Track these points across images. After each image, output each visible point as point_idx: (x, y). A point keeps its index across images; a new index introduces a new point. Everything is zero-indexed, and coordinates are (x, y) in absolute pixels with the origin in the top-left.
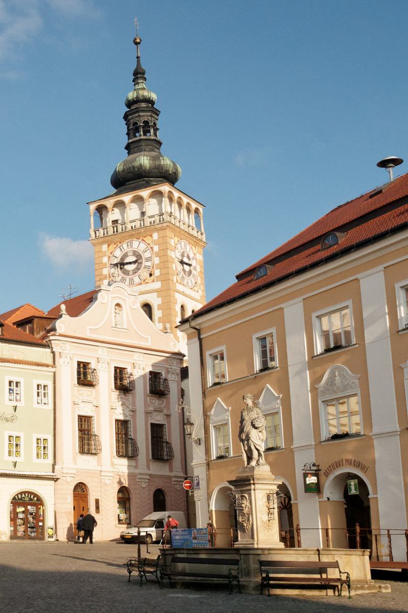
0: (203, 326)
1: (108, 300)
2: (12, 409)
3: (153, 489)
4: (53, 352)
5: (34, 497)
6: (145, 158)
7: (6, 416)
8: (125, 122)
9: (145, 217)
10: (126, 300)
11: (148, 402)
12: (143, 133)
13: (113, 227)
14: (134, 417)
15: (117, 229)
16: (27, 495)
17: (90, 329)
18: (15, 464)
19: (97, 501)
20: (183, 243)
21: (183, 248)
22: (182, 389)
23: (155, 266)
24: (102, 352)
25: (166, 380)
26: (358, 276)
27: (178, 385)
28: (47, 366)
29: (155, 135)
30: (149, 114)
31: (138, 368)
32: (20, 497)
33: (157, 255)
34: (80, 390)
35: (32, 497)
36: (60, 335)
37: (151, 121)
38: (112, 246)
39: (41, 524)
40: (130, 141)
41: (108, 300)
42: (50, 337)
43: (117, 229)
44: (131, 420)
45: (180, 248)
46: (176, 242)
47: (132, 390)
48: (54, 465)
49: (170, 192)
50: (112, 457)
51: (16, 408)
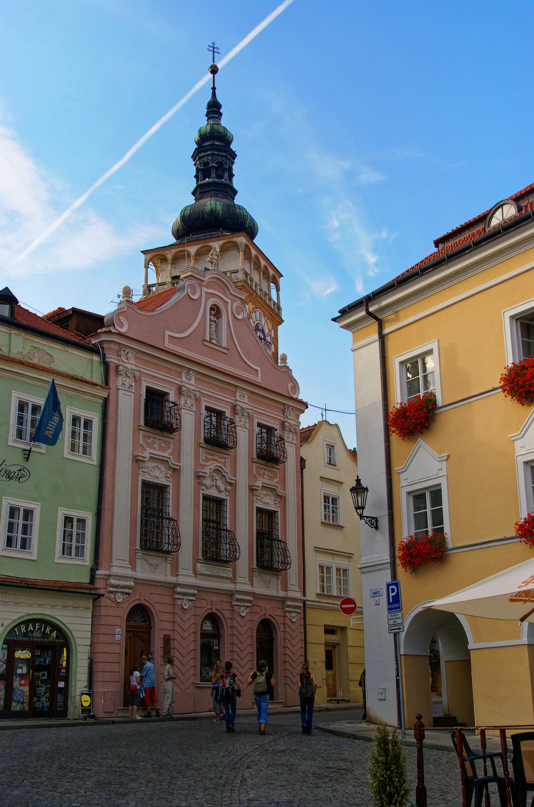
2: (19, 458)
3: (257, 619)
4: (106, 365)
5: (51, 631)
6: (218, 203)
7: (8, 469)
8: (194, 163)
10: (227, 303)
11: (254, 473)
12: (216, 176)
16: (37, 627)
17: (169, 336)
19: (167, 640)
20: (258, 313)
21: (258, 319)
22: (301, 458)
25: (282, 439)
27: (298, 452)
31: (240, 414)
32: (23, 630)
34: (149, 438)
35: (48, 630)
36: (120, 334)
37: (226, 163)
39: (61, 684)
42: (102, 335)
44: (228, 498)
45: (254, 317)
46: (251, 310)
47: (231, 448)
48: (93, 571)
49: (246, 246)
50: (196, 560)
51: (29, 455)
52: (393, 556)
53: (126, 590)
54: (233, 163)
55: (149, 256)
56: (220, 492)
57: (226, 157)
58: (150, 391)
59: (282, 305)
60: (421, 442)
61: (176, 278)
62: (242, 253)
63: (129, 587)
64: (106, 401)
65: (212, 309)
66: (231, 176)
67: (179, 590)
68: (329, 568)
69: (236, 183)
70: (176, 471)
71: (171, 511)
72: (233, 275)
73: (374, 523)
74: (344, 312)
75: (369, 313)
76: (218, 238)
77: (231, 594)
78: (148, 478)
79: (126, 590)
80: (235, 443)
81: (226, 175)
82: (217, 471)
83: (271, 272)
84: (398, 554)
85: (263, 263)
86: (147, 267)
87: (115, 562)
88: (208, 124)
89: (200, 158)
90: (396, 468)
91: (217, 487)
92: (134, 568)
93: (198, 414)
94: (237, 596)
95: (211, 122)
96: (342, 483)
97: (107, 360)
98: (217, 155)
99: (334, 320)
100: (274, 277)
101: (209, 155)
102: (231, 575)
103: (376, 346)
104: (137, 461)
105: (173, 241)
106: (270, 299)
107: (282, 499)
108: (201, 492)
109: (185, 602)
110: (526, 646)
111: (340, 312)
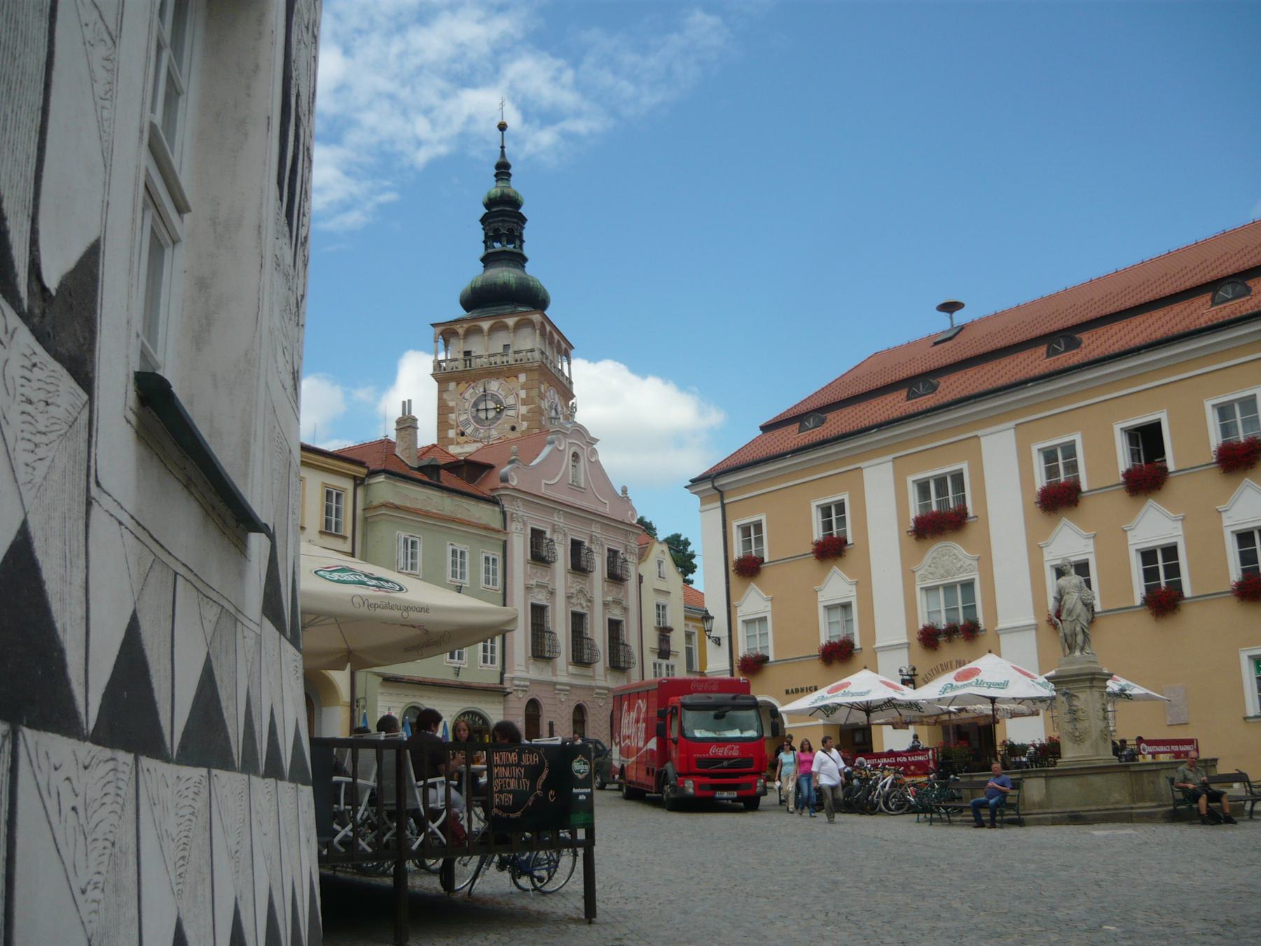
0: (727, 488)
1: (565, 448)
4: (504, 513)
5: (479, 720)
9: (511, 351)
13: (466, 361)
14: (591, 608)
15: (470, 364)
18: (458, 671)
19: (551, 725)
23: (520, 417)
24: (559, 520)
26: (979, 433)
27: (637, 569)
28: (499, 531)
29: (521, 247)
30: (515, 220)
33: (524, 402)
36: (515, 489)
37: (517, 230)
38: (463, 385)
40: (490, 251)
41: (565, 448)
43: (470, 364)
48: (502, 674)
52: (732, 665)
53: (525, 689)
54: (523, 228)
55: (439, 329)
56: (583, 608)
57: (517, 224)
58: (533, 530)
59: (573, 380)
60: (753, 585)
61: (467, 353)
62: (538, 332)
63: (527, 687)
64: (505, 542)
65: (573, 456)
66: (522, 241)
67: (558, 687)
68: (660, 665)
69: (527, 250)
70: (552, 593)
71: (550, 625)
72: (529, 354)
73: (718, 641)
74: (696, 481)
75: (715, 488)
76: (512, 314)
77: (591, 688)
78: (535, 601)
79: (525, 689)
80: (594, 567)
81: (518, 242)
82: (581, 591)
83: (564, 346)
84: (735, 665)
85: (556, 336)
86: (436, 341)
87: (517, 668)
88: (497, 187)
89: (490, 224)
90: (734, 603)
91: (581, 605)
92: (528, 672)
93: (566, 546)
94: (598, 691)
95: (500, 184)
96: (669, 593)
97: (505, 509)
98: (508, 221)
99: (686, 487)
100: (566, 350)
101: (499, 221)
102: (592, 674)
103: (719, 511)
104: (528, 588)
105: (461, 313)
106: (563, 374)
107: (626, 609)
108: (570, 609)
109: (562, 696)
110: (822, 727)
111: (691, 481)
